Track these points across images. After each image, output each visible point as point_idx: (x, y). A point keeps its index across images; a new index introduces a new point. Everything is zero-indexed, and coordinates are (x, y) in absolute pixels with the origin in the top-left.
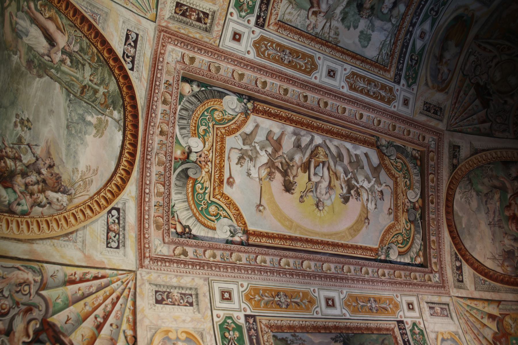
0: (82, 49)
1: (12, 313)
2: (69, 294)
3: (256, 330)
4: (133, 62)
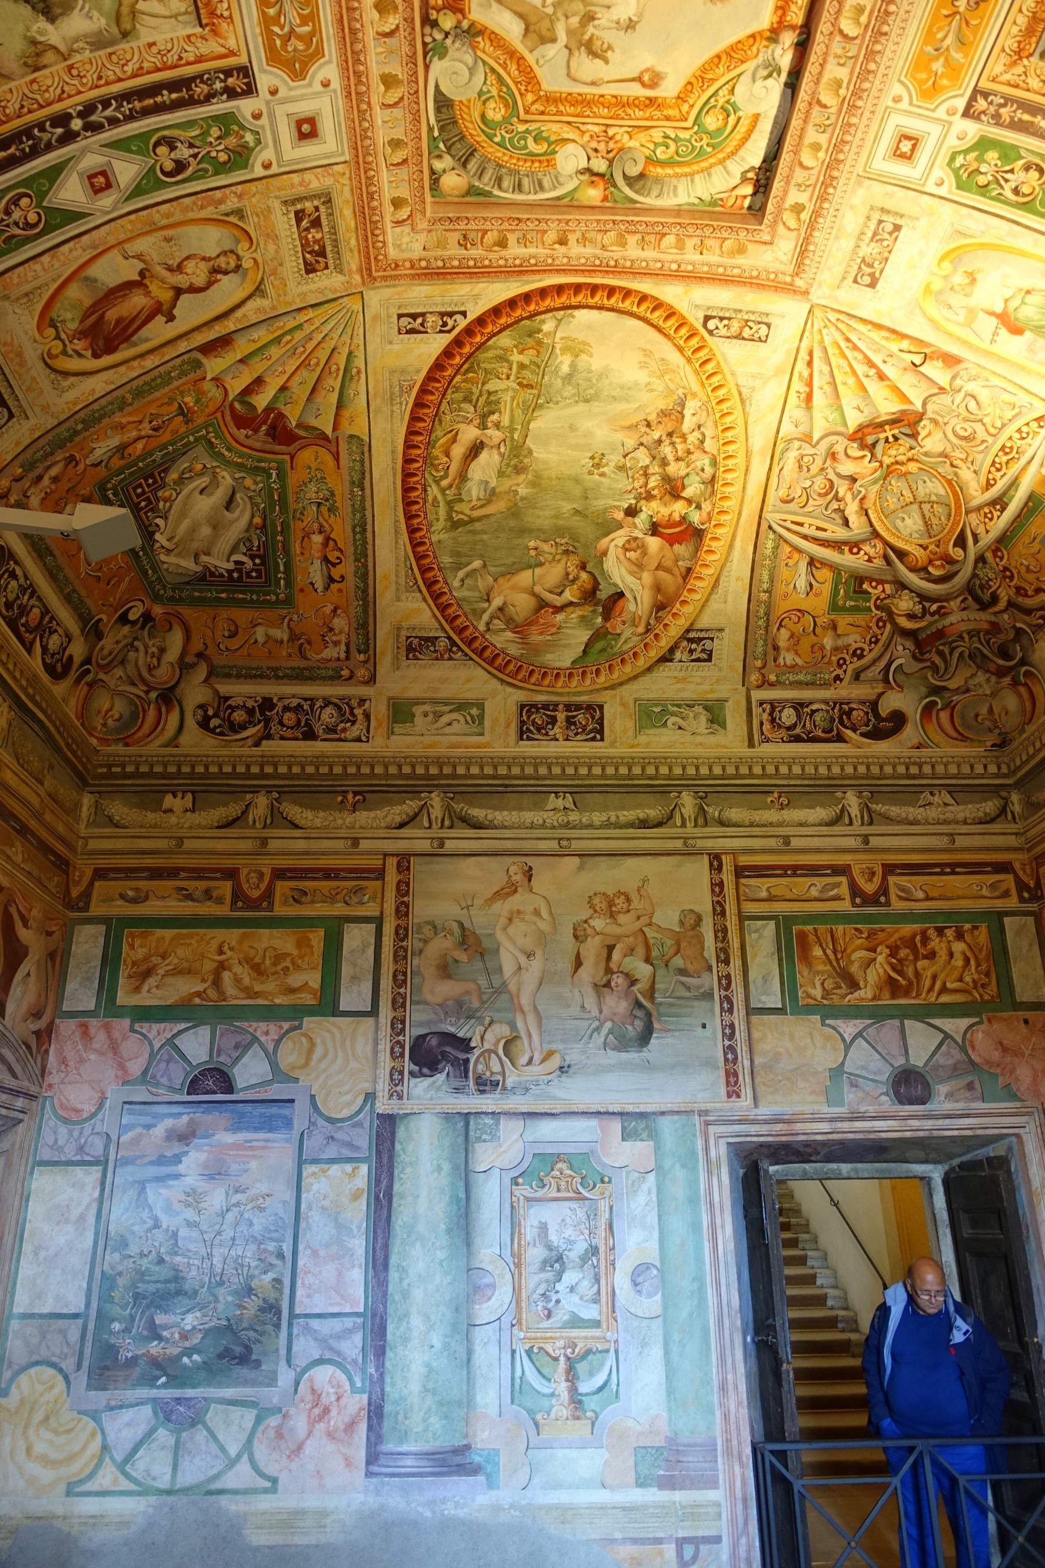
0: (467, 399)
1: (832, 476)
2: (825, 402)
3: (1008, 100)
4: (451, 314)
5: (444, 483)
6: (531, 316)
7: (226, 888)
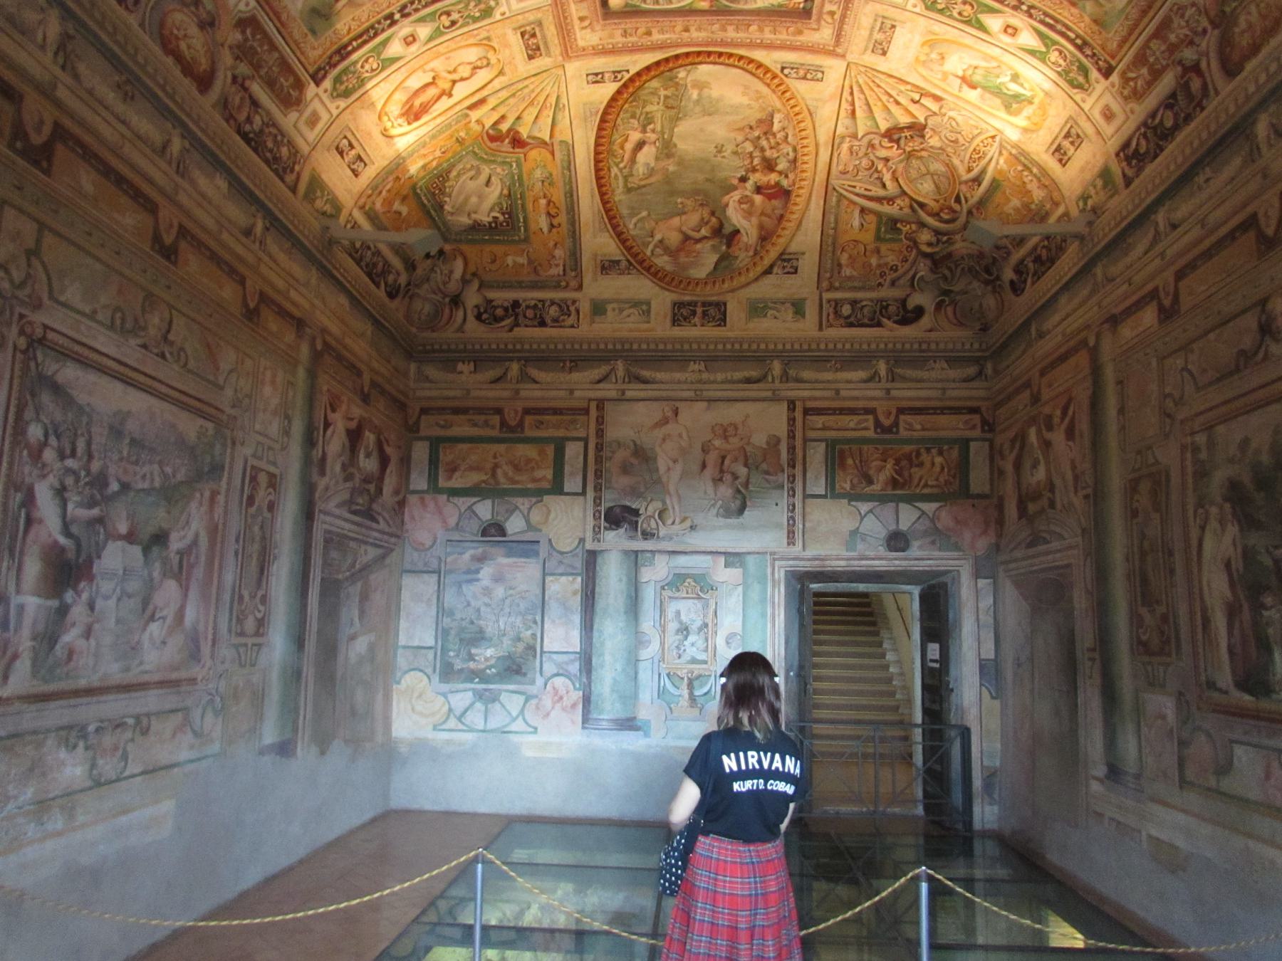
0: (633, 116)
1: (872, 157)
5: (621, 165)
6: (670, 70)
7: (496, 419)
